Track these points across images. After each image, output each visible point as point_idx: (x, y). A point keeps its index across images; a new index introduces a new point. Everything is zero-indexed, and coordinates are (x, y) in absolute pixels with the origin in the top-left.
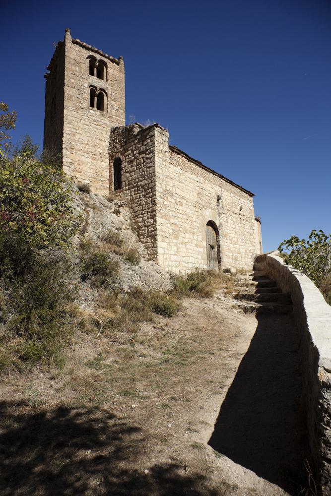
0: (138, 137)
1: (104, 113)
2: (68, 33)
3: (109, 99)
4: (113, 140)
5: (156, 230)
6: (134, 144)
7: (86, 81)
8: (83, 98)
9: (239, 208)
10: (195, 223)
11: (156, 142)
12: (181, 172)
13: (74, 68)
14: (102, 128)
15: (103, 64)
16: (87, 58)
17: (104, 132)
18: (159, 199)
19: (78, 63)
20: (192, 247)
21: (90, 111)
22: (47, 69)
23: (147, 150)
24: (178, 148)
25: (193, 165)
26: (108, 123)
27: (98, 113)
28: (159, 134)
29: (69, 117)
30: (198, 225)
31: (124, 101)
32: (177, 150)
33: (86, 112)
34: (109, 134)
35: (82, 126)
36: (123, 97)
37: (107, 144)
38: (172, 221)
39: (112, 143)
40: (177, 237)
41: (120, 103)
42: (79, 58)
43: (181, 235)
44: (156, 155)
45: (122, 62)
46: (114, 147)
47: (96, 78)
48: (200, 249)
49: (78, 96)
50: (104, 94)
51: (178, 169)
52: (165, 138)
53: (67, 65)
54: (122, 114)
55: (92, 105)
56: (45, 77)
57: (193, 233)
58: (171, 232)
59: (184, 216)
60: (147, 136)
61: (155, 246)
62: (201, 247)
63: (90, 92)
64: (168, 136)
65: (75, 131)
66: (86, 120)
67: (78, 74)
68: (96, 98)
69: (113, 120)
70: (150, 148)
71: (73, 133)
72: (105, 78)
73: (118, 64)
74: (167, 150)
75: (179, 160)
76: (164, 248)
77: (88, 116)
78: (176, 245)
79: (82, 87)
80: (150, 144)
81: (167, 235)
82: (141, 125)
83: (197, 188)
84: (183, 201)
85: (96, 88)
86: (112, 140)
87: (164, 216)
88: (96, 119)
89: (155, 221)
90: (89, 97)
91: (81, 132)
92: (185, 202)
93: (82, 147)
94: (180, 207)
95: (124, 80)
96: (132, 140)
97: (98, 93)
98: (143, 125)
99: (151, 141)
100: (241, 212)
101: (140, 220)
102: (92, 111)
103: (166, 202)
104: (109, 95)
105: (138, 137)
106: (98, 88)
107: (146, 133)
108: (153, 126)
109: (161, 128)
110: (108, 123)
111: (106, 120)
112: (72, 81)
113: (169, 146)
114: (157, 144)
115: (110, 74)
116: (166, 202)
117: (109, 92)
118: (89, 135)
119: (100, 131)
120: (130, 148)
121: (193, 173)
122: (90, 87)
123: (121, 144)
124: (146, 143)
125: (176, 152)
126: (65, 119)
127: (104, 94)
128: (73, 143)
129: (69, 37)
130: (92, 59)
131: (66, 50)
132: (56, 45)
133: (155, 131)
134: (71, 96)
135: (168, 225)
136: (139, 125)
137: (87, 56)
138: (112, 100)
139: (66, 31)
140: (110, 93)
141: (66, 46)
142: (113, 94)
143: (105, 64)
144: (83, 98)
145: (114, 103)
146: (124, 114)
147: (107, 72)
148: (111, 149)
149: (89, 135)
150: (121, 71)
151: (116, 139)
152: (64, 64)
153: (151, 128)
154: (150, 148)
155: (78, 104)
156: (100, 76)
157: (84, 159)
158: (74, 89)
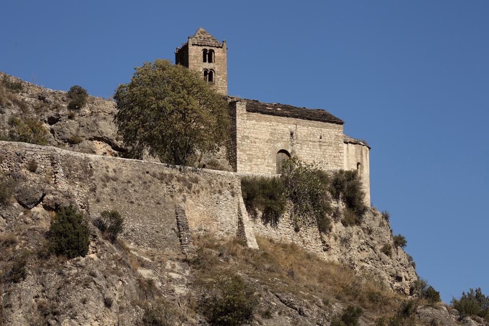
5: (236, 158)
9: (319, 137)
10: (266, 153)
12: (256, 123)
13: (194, 62)
15: (212, 51)
18: (238, 141)
20: (264, 166)
25: (267, 116)
30: (269, 153)
38: (248, 152)
40: (251, 161)
43: (254, 160)
48: (270, 168)
51: (253, 122)
53: (190, 62)
54: (225, 82)
57: (265, 159)
58: (246, 158)
59: (257, 149)
61: (236, 167)
62: (271, 167)
74: (246, 112)
75: (254, 116)
76: (241, 167)
78: (251, 165)
81: (244, 161)
83: (270, 130)
84: (256, 140)
87: (242, 150)
89: (236, 153)
92: (259, 141)
94: (255, 144)
100: (321, 140)
101: (230, 153)
103: (243, 143)
104: (216, 72)
116: (243, 143)
117: (216, 70)
130: (205, 51)
135: (245, 155)
138: (218, 74)
143: (213, 51)
145: (219, 76)
156: (210, 61)
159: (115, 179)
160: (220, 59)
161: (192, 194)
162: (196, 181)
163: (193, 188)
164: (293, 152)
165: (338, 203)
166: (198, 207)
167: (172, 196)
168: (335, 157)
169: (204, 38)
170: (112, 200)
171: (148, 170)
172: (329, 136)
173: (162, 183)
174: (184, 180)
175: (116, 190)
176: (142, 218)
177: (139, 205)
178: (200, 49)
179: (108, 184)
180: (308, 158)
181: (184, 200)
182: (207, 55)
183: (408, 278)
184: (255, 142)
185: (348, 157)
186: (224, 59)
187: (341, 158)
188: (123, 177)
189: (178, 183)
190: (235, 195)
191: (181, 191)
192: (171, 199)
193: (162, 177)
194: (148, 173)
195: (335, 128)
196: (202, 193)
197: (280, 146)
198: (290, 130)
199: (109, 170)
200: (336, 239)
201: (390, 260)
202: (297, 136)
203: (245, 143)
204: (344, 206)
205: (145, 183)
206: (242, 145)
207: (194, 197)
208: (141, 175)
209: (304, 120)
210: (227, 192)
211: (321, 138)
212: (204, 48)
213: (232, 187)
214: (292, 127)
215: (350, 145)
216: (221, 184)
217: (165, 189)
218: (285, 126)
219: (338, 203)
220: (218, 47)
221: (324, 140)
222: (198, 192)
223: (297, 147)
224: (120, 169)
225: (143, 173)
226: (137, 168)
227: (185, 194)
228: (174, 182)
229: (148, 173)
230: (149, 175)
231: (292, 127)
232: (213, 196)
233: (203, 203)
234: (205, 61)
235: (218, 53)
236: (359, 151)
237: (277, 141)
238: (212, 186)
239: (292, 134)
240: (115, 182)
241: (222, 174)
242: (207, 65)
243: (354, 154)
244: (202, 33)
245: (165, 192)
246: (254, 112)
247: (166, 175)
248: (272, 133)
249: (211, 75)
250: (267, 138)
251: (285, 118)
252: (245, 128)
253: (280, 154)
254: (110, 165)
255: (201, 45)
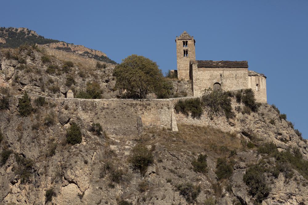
9: (235, 75)
12: (203, 72)
15: (187, 42)
18: (194, 81)
25: (208, 69)
38: (199, 86)
58: (198, 88)
93: (182, 68)
103: (196, 82)
116: (196, 82)
117: (189, 50)
121: (208, 70)
130: (184, 42)
138: (190, 52)
157: (183, 72)
159: (108, 108)
160: (190, 44)
161: (147, 110)
162: (149, 105)
163: (147, 108)
164: (222, 83)
165: (240, 104)
166: (150, 116)
167: (136, 113)
168: (243, 83)
169: (184, 36)
170: (105, 117)
171: (124, 103)
172: (240, 74)
173: (131, 107)
174: (143, 105)
175: (108, 113)
176: (120, 124)
177: (119, 118)
178: (181, 41)
179: (104, 111)
180: (230, 85)
181: (143, 114)
183: (288, 133)
184: (202, 81)
185: (251, 82)
186: (192, 45)
187: (247, 83)
188: (112, 107)
189: (140, 106)
190: (170, 109)
191: (141, 110)
192: (135, 114)
193: (132, 105)
194: (124, 104)
195: (244, 70)
196: (152, 109)
197: (215, 81)
198: (220, 73)
199: (105, 105)
200: (238, 120)
201: (274, 126)
202: (224, 76)
203: (197, 82)
204: (244, 105)
205: (123, 108)
206: (196, 83)
207: (148, 112)
208: (121, 105)
209: (227, 68)
210: (165, 108)
211: (236, 75)
212: (183, 40)
213: (168, 105)
214: (221, 72)
215: (252, 76)
216: (162, 105)
217: (133, 110)
218: (217, 72)
219: (240, 104)
220: (189, 40)
221: (238, 76)
222: (150, 109)
223: (224, 81)
224: (110, 104)
225: (122, 104)
226: (119, 102)
227: (144, 111)
228: (137, 106)
229: (124, 104)
230: (125, 105)
231: (221, 72)
232: (158, 110)
233: (153, 114)
235: (190, 42)
236: (257, 79)
237: (214, 79)
238: (158, 106)
239: (221, 75)
240: (107, 110)
241: (163, 100)
242: (185, 48)
243: (255, 80)
244: (184, 34)
245: (133, 111)
246: (201, 67)
247: (133, 104)
248: (211, 76)
249: (187, 52)
250: (209, 78)
251: (217, 69)
252: (197, 75)
253: (216, 85)
254: (105, 103)
255: (182, 40)
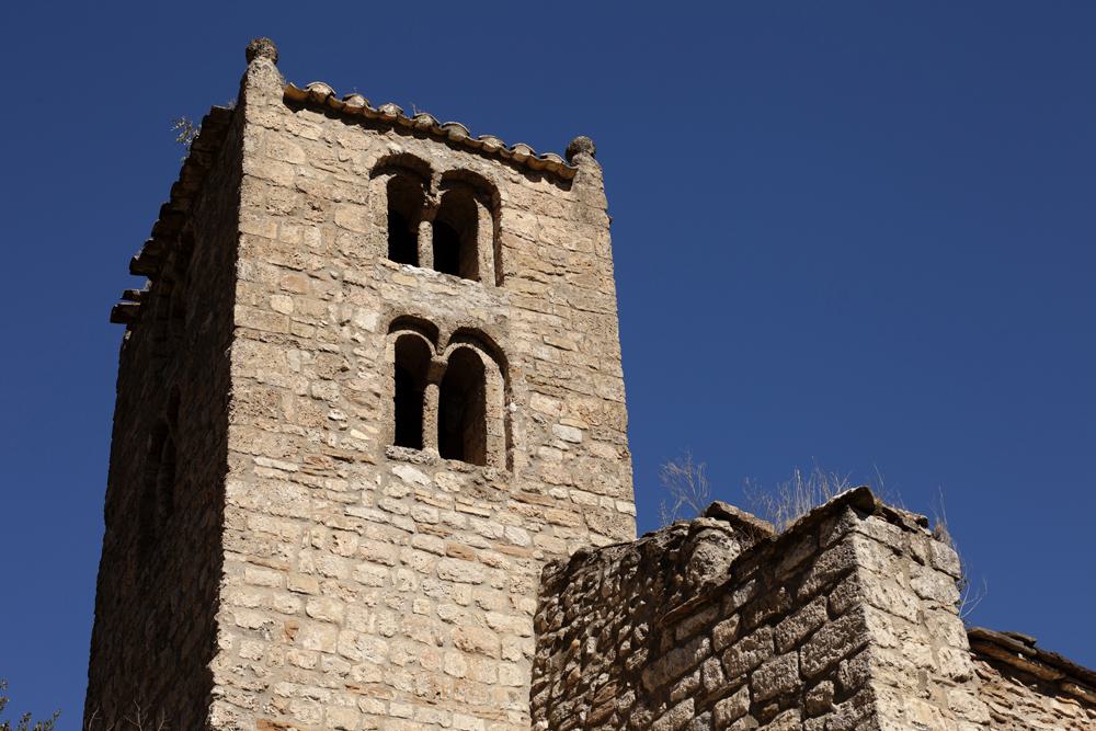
0: (739, 598)
1: (492, 472)
2: (263, 61)
3: (520, 387)
4: (562, 644)
6: (713, 652)
7: (368, 296)
8: (353, 397)
11: (872, 620)
13: (291, 234)
14: (475, 571)
15: (472, 192)
16: (375, 172)
17: (490, 598)
19: (317, 206)
21: (397, 469)
22: (135, 268)
23: (810, 680)
24: (1046, 646)
26: (519, 536)
27: (451, 476)
28: (884, 557)
29: (258, 523)
31: (613, 387)
32: (1038, 658)
33: (373, 478)
34: (531, 604)
35: (341, 572)
36: (607, 366)
37: (520, 675)
39: (554, 660)
41: (591, 404)
42: (322, 176)
44: (881, 705)
45: (589, 167)
46: (572, 687)
47: (430, 271)
49: (318, 390)
50: (486, 359)
52: (928, 582)
53: (251, 223)
54: (608, 468)
55: (408, 433)
56: (118, 315)
60: (798, 580)
63: (391, 357)
64: (955, 568)
65: (296, 604)
66: (372, 529)
67: (315, 262)
68: (432, 393)
69: (550, 514)
70: (835, 666)
71: (281, 622)
72: (486, 266)
73: (563, 180)
74: (963, 663)
77: (385, 502)
79: (346, 331)
80: (829, 633)
82: (748, 516)
85: (430, 329)
86: (555, 640)
88: (434, 514)
90: (386, 386)
91: (336, 611)
95: (607, 268)
96: (690, 623)
97: (444, 359)
98: (761, 514)
99: (833, 615)
102: (408, 472)
104: (515, 362)
105: (739, 598)
106: (445, 332)
107: (792, 562)
108: (837, 510)
109: (892, 518)
110: (519, 536)
111: (502, 514)
112: (283, 304)
113: (975, 639)
114: (878, 630)
115: (521, 244)
117: (518, 342)
118: (389, 623)
119: (466, 594)
120: (686, 682)
122: (393, 327)
123: (620, 661)
124: (794, 629)
125: (1028, 679)
126: (230, 539)
127: (486, 359)
128: (285, 688)
129: (266, 79)
130: (404, 176)
131: (249, 145)
132: (187, 132)
133: (857, 539)
134: (274, 395)
136: (734, 520)
137: (372, 162)
138: (540, 388)
139: (251, 55)
140: (523, 347)
141: (249, 130)
142: (544, 353)
143: (487, 193)
144: (353, 397)
145: (548, 405)
146: (625, 468)
147: (498, 231)
148: (549, 704)
149: (389, 623)
150: (586, 218)
151: (579, 632)
152: (236, 222)
153: (823, 526)
154: (835, 666)
155: (315, 436)
156: (456, 258)
158: (293, 353)
178: (370, 147)
182: (425, 227)
212: (398, 144)
234: (403, 250)
